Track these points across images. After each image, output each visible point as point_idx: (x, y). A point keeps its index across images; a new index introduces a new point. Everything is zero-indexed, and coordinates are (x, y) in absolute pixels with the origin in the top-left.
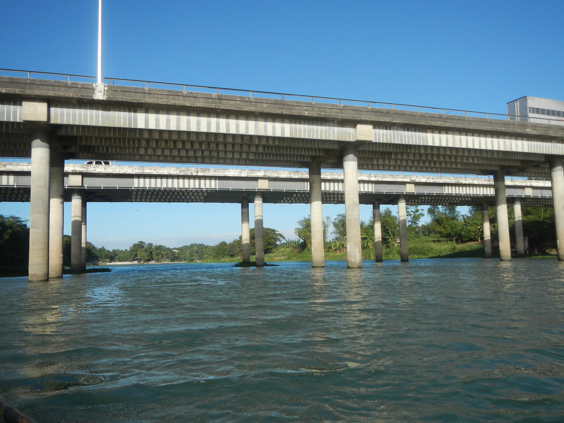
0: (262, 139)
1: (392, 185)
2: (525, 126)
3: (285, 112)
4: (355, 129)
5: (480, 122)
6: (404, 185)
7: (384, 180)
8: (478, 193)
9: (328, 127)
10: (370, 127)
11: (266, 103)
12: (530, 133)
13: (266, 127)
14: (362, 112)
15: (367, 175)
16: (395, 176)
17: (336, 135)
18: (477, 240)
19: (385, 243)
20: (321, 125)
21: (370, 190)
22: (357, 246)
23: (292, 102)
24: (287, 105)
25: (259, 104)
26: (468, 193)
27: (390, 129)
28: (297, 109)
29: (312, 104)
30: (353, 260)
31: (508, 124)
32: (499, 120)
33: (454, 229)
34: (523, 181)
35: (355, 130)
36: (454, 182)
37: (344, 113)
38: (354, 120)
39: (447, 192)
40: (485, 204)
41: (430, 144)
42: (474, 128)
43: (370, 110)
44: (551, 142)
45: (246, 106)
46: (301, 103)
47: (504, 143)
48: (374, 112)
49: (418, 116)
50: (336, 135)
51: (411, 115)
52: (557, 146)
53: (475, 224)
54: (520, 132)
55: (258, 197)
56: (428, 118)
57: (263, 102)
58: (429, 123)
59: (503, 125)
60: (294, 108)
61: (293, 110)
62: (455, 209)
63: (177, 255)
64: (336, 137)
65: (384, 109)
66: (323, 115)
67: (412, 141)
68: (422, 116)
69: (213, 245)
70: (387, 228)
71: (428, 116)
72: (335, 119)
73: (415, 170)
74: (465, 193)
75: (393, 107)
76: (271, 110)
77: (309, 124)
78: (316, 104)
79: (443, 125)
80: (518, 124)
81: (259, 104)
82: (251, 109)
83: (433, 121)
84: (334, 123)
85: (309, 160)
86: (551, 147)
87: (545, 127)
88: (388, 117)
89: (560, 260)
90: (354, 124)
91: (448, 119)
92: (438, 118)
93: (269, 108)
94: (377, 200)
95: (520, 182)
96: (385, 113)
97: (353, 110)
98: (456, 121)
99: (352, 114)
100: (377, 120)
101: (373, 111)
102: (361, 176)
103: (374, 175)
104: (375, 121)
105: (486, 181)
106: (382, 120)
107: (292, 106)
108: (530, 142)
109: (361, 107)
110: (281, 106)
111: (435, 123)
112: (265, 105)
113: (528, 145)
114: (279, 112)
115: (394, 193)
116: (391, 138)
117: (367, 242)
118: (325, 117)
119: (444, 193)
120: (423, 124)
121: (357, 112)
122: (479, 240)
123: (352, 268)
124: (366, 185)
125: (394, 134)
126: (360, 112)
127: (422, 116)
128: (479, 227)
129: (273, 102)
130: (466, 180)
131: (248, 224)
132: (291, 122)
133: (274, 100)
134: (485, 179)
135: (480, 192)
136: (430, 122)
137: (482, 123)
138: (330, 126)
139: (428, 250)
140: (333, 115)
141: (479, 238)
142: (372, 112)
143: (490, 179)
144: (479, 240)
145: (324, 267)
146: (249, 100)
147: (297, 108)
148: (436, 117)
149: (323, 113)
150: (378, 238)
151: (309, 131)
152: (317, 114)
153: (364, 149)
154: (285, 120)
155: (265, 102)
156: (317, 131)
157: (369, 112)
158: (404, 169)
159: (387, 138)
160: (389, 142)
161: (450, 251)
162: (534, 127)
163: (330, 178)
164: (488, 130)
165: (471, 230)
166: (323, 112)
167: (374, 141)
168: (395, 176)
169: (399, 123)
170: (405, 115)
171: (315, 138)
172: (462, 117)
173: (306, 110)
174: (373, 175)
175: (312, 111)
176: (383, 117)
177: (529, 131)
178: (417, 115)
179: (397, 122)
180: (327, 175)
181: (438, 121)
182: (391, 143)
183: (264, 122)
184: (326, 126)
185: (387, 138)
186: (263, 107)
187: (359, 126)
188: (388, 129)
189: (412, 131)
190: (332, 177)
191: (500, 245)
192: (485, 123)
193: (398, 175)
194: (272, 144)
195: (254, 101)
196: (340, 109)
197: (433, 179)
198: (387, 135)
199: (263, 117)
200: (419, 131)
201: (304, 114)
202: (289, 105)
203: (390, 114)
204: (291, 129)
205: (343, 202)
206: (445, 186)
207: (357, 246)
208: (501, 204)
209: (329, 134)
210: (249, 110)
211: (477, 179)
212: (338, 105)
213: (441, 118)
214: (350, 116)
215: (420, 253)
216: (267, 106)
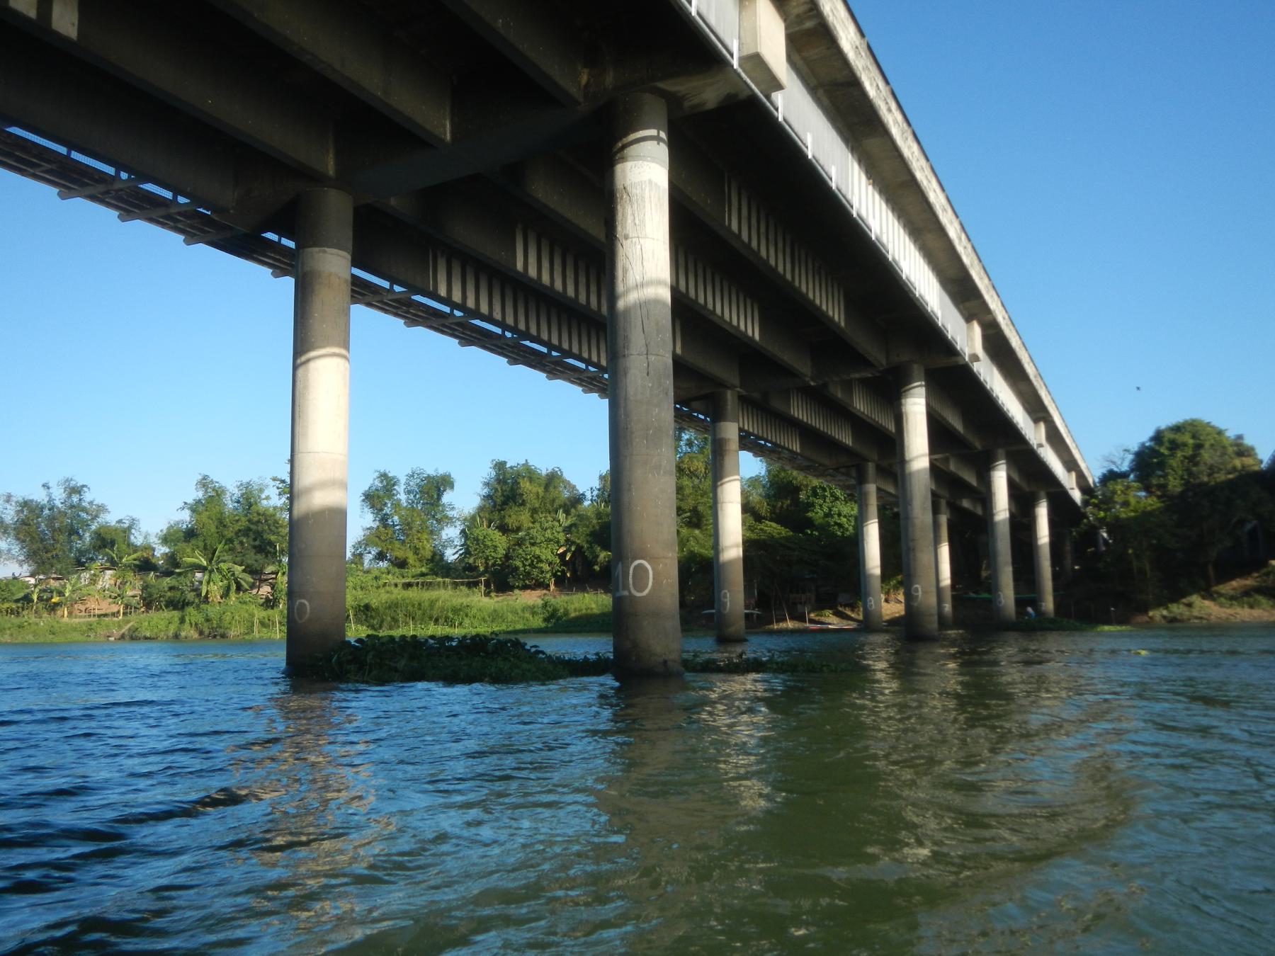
18: (547, 587)
53: (549, 540)
55: (658, 139)
70: (273, 538)
122: (552, 587)
128: (561, 551)
131: (347, 364)
139: (456, 611)
141: (553, 580)
144: (552, 587)
165: (543, 557)
215: (431, 618)
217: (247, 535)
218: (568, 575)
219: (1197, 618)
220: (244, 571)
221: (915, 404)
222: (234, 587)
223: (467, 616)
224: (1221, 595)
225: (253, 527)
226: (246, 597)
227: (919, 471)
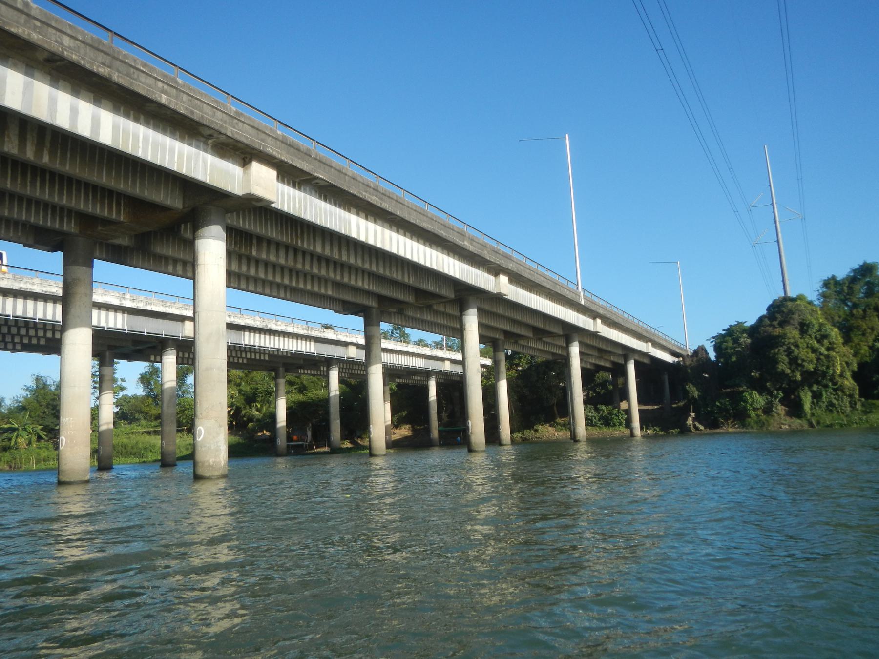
0: (6, 139)
1: (161, 320)
2: (463, 235)
3: (118, 76)
4: (246, 169)
5: (420, 213)
6: (180, 323)
7: (149, 308)
8: (290, 348)
9: (193, 150)
10: (272, 173)
11: (71, 37)
12: (468, 248)
13: (53, 102)
14: (267, 137)
15: (118, 295)
16: (169, 304)
17: (208, 172)
19: (51, 439)
20: (182, 139)
21: (119, 326)
22: (222, 429)
23: (135, 61)
24: (122, 61)
25: (54, 31)
26: (277, 346)
27: (300, 189)
28: (143, 80)
29: (177, 82)
30: (211, 461)
31: (448, 227)
33: (186, 412)
34: (348, 334)
35: (244, 172)
36: (260, 326)
37: (236, 126)
38: (253, 149)
39: (247, 343)
40: (281, 369)
41: (354, 235)
42: (414, 222)
43: (281, 138)
45: (17, 22)
46: (152, 69)
47: (437, 257)
48: (286, 144)
49: (349, 176)
50: (208, 172)
51: (339, 171)
54: (459, 244)
56: (361, 184)
57: (64, 30)
58: (362, 194)
59: (443, 227)
60: (138, 76)
61: (134, 79)
62: (186, 377)
64: (208, 177)
65: (303, 145)
66: (197, 115)
67: (331, 222)
68: (354, 179)
71: (362, 181)
72: (216, 135)
73: (253, 290)
74: (272, 346)
75: (313, 146)
76: (83, 59)
77: (156, 128)
78: (184, 86)
79: (379, 205)
80: (457, 230)
81: (50, 30)
82: (29, 34)
83: (366, 192)
84: (206, 144)
85: (70, 227)
87: (481, 244)
88: (307, 162)
89: (470, 450)
90: (244, 159)
91: (385, 195)
92: (374, 189)
93: (79, 52)
94: (111, 347)
95: (344, 336)
96: (302, 152)
97: (253, 127)
98: (394, 202)
99: (250, 135)
100: (290, 162)
101: (284, 141)
102: (105, 295)
103: (131, 296)
104: (286, 163)
105: (303, 329)
106: (298, 166)
107: (132, 70)
109: (266, 127)
110: (108, 60)
111: (369, 197)
112: (67, 41)
114: (103, 71)
115: (163, 336)
116: (300, 207)
117: (17, 437)
118: (201, 121)
119: (243, 343)
120: (355, 193)
121: (258, 134)
123: (209, 478)
124: (111, 314)
125: (305, 199)
126: (263, 136)
127: (354, 179)
129: (89, 42)
130: (277, 325)
132: (116, 110)
133: (92, 37)
134: (302, 326)
135: (293, 347)
136: (364, 193)
137: (422, 216)
138: (198, 147)
139: (146, 448)
140: (217, 123)
142: (282, 142)
143: (308, 327)
145: (87, 482)
146: (26, 10)
147: (143, 78)
148: (370, 187)
149: (198, 112)
150: (108, 423)
151: (155, 144)
152: (186, 109)
153: (229, 221)
154: (103, 101)
155: (69, 31)
156: (172, 151)
157: (278, 142)
158: (236, 286)
159: (294, 204)
160: (297, 214)
161: (187, 449)
163: (40, 292)
164: (429, 230)
166: (197, 109)
167: (273, 205)
168: (169, 304)
169: (323, 179)
170: (331, 167)
171: (166, 165)
172: (400, 198)
173: (166, 93)
174: (128, 296)
175: (177, 98)
176: (299, 158)
177: (466, 246)
178: (348, 173)
179: (321, 176)
180: (33, 284)
181: (373, 195)
182: (300, 216)
183: (51, 85)
184: (190, 145)
185: (294, 204)
186: (62, 44)
187: (256, 166)
188: (297, 188)
189: (330, 203)
190: (45, 289)
191: (371, 430)
192: (425, 218)
193: (174, 303)
194: (32, 158)
195: (39, 17)
196: (230, 116)
197: (229, 316)
198: (294, 198)
199: (49, 74)
200: (340, 207)
201: (159, 99)
202: (126, 63)
203: (309, 157)
204: (116, 128)
205: (227, 324)
206: (244, 331)
207: (222, 429)
208: (376, 364)
209: (195, 164)
210: (25, 36)
211: (293, 325)
212: (226, 105)
213: (377, 191)
214: (247, 138)
215: (131, 454)
216: (72, 45)
217: (48, 408)
218: (234, 423)
219: (536, 438)
220: (41, 429)
221: (167, 358)
222: (34, 438)
223: (151, 451)
224: (558, 424)
225: (51, 402)
226: (43, 443)
227: (166, 389)
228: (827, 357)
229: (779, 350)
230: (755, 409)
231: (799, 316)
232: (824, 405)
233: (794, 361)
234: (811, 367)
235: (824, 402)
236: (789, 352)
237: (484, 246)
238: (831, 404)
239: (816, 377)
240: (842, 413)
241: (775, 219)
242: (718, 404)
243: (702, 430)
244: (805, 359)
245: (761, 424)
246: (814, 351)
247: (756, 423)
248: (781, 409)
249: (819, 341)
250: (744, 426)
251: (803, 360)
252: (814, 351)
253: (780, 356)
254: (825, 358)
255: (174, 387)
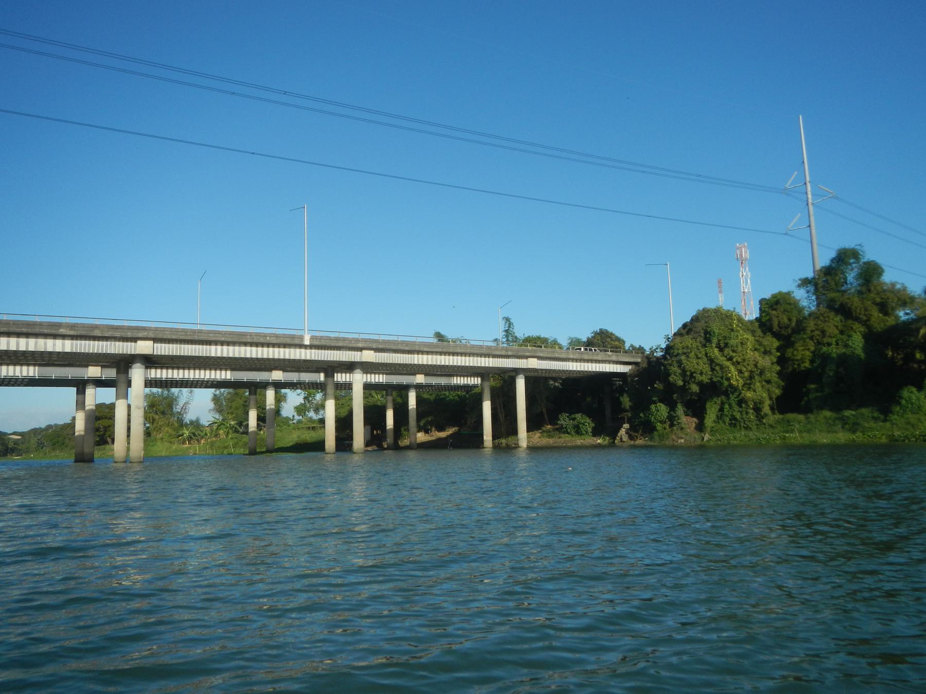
21: (31, 374)
32: (18, 321)
39: (153, 376)
44: (107, 341)
52: (115, 345)
63: (11, 445)
69: (26, 431)
86: (107, 346)
108: (75, 342)
113: (72, 345)
150: (80, 431)
162: (72, 326)
228: (722, 367)
229: (673, 361)
230: (661, 422)
231: (706, 323)
232: (727, 420)
233: (684, 371)
234: (705, 379)
235: (727, 416)
236: (680, 363)
237: (96, 327)
238: (735, 419)
239: (713, 389)
240: (744, 427)
241: (807, 201)
242: (642, 415)
243: (624, 442)
244: (693, 370)
245: (662, 437)
246: (711, 361)
247: (659, 436)
248: (688, 422)
249: (721, 350)
250: (651, 439)
251: (692, 373)
252: (711, 361)
253: (672, 367)
254: (721, 369)
255: (92, 410)
